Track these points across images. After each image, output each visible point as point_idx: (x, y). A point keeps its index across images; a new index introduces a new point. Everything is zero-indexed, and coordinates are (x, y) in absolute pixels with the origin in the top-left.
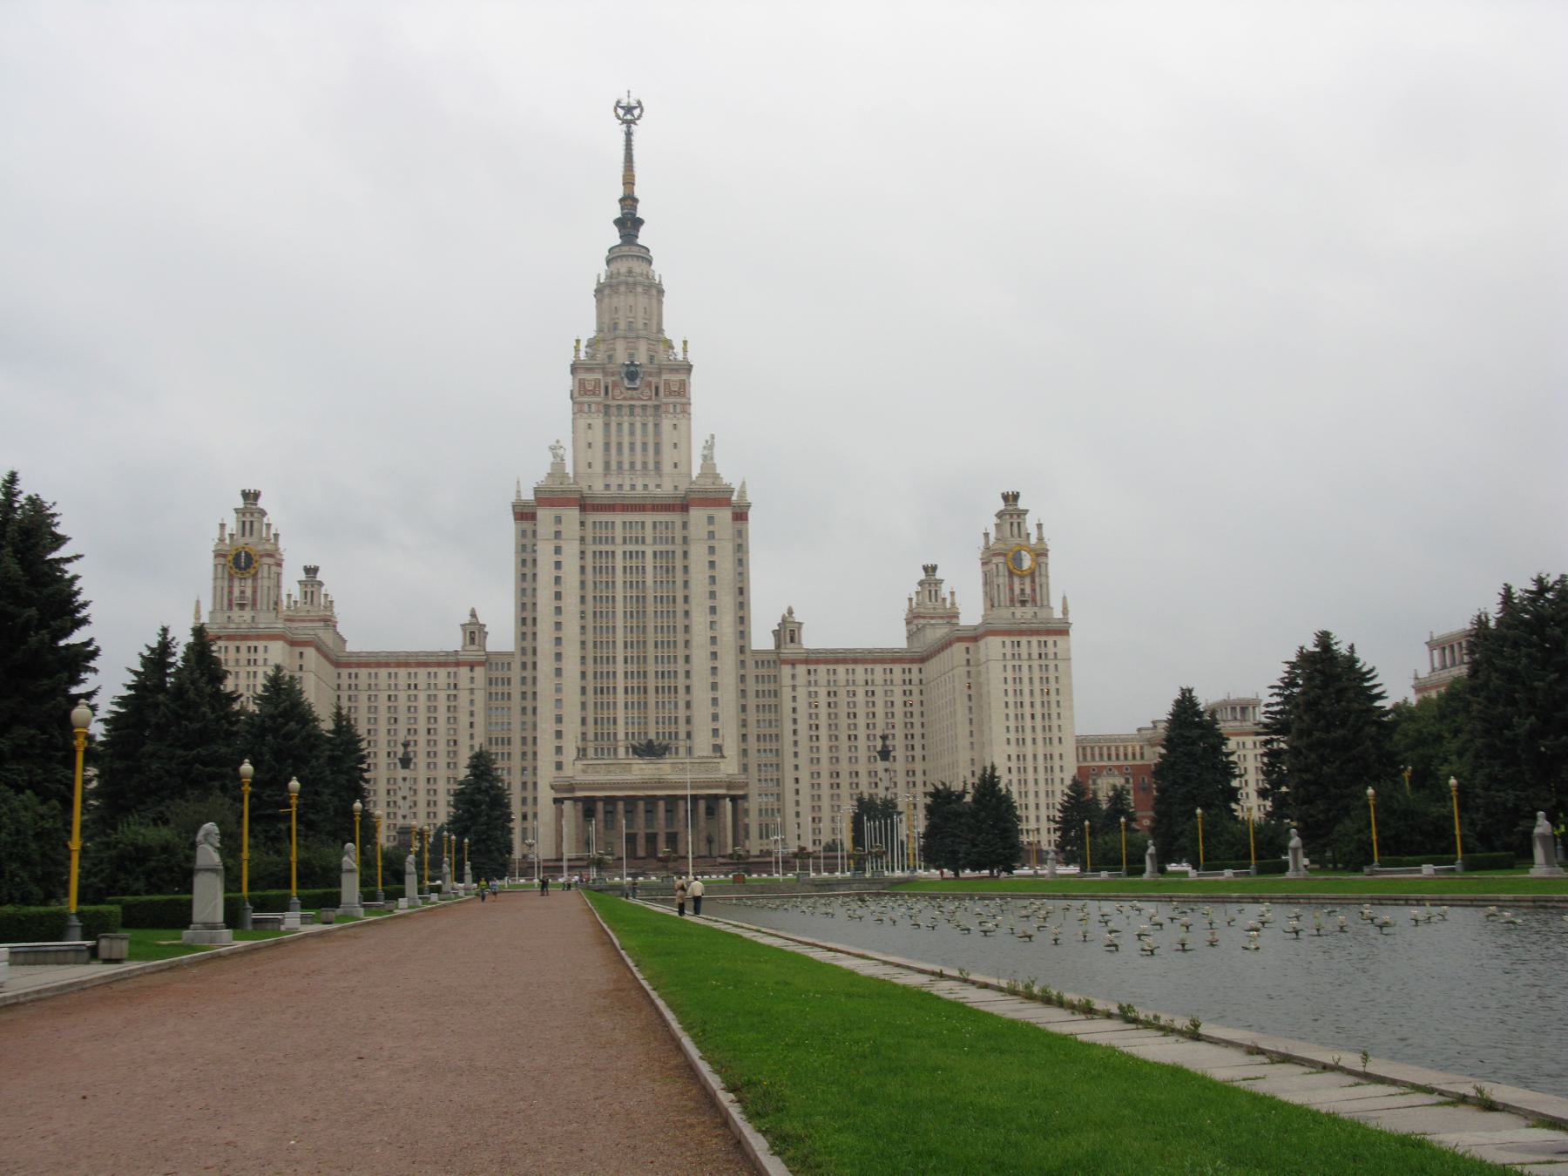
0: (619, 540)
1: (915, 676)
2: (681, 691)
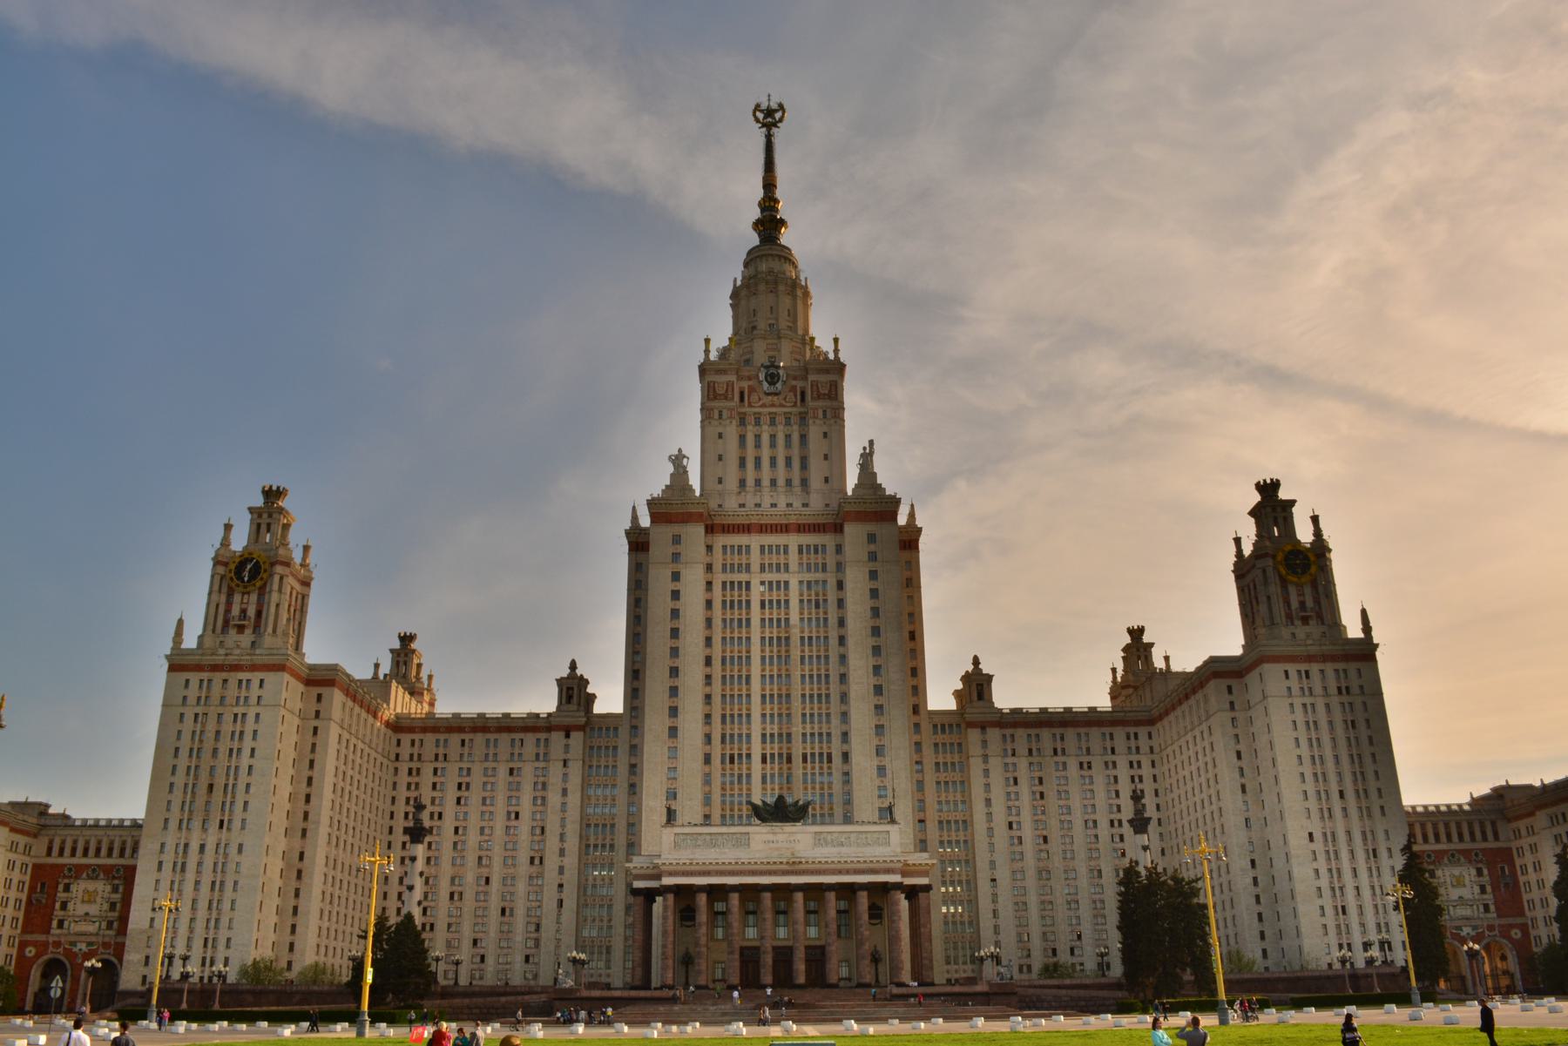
0: (755, 567)
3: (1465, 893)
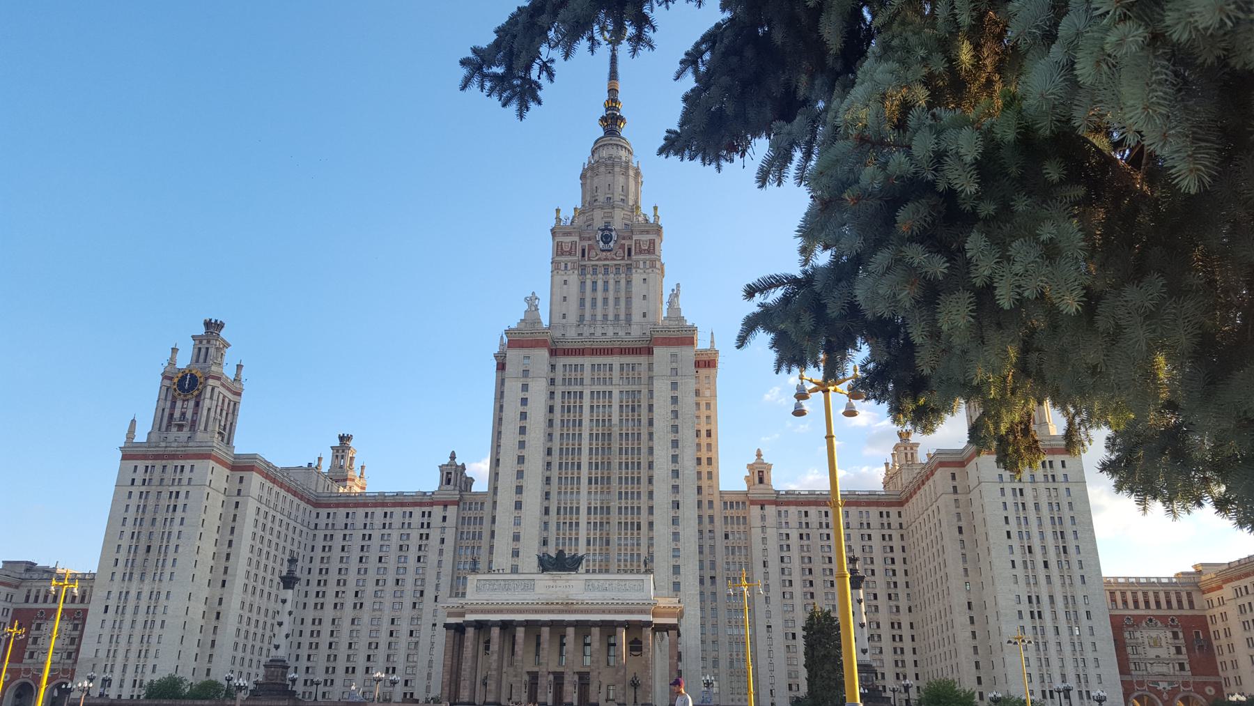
1: (894, 519)
2: (644, 527)
3: (1163, 653)
